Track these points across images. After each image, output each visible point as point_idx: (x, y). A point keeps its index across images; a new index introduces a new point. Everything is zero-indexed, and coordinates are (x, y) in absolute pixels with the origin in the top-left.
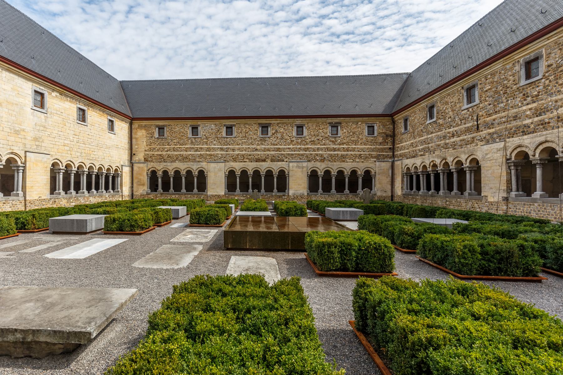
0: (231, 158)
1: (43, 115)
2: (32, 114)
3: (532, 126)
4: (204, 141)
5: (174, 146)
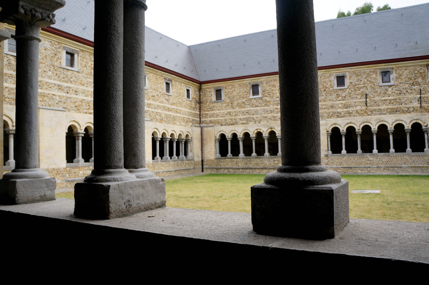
3: (343, 113)
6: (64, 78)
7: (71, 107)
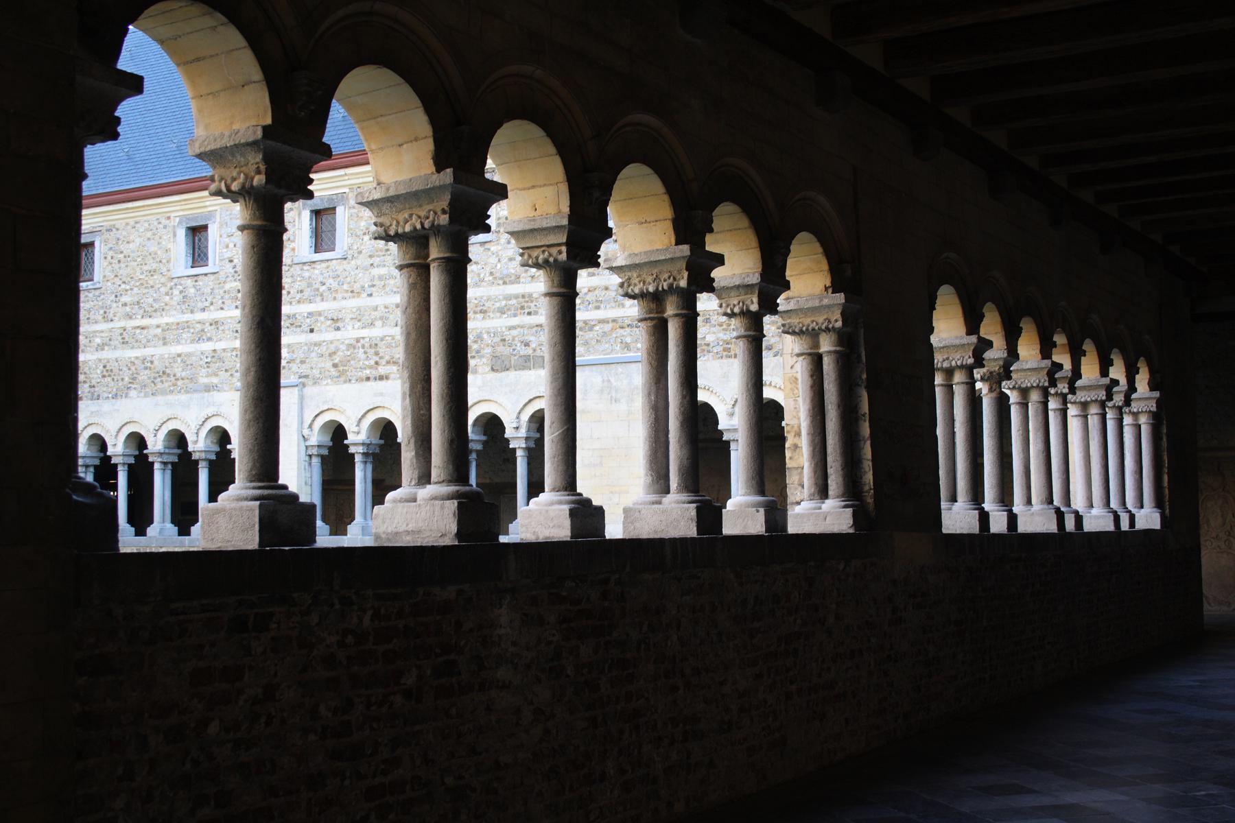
0: (329, 365)
4: (227, 286)
5: (122, 324)
6: (302, 291)
7: (323, 370)
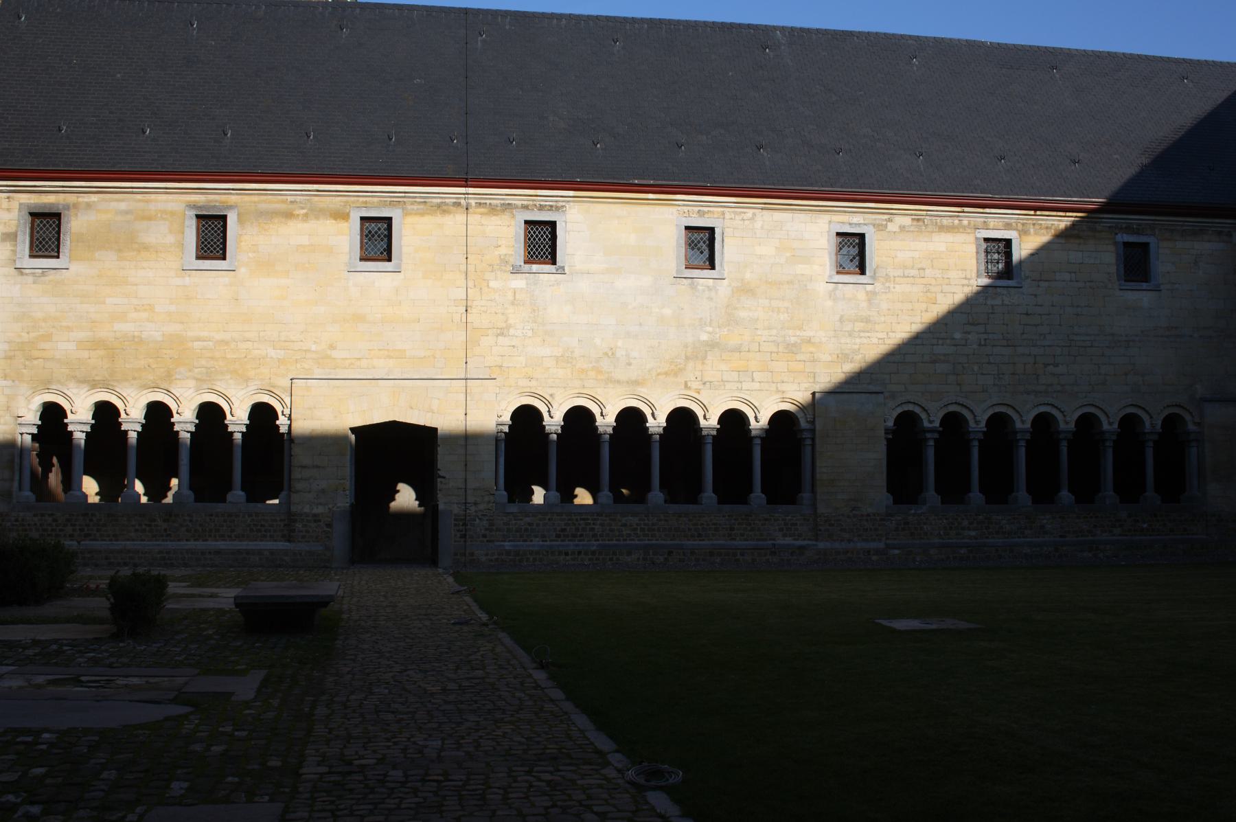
1: (861, 294)
2: (832, 295)
